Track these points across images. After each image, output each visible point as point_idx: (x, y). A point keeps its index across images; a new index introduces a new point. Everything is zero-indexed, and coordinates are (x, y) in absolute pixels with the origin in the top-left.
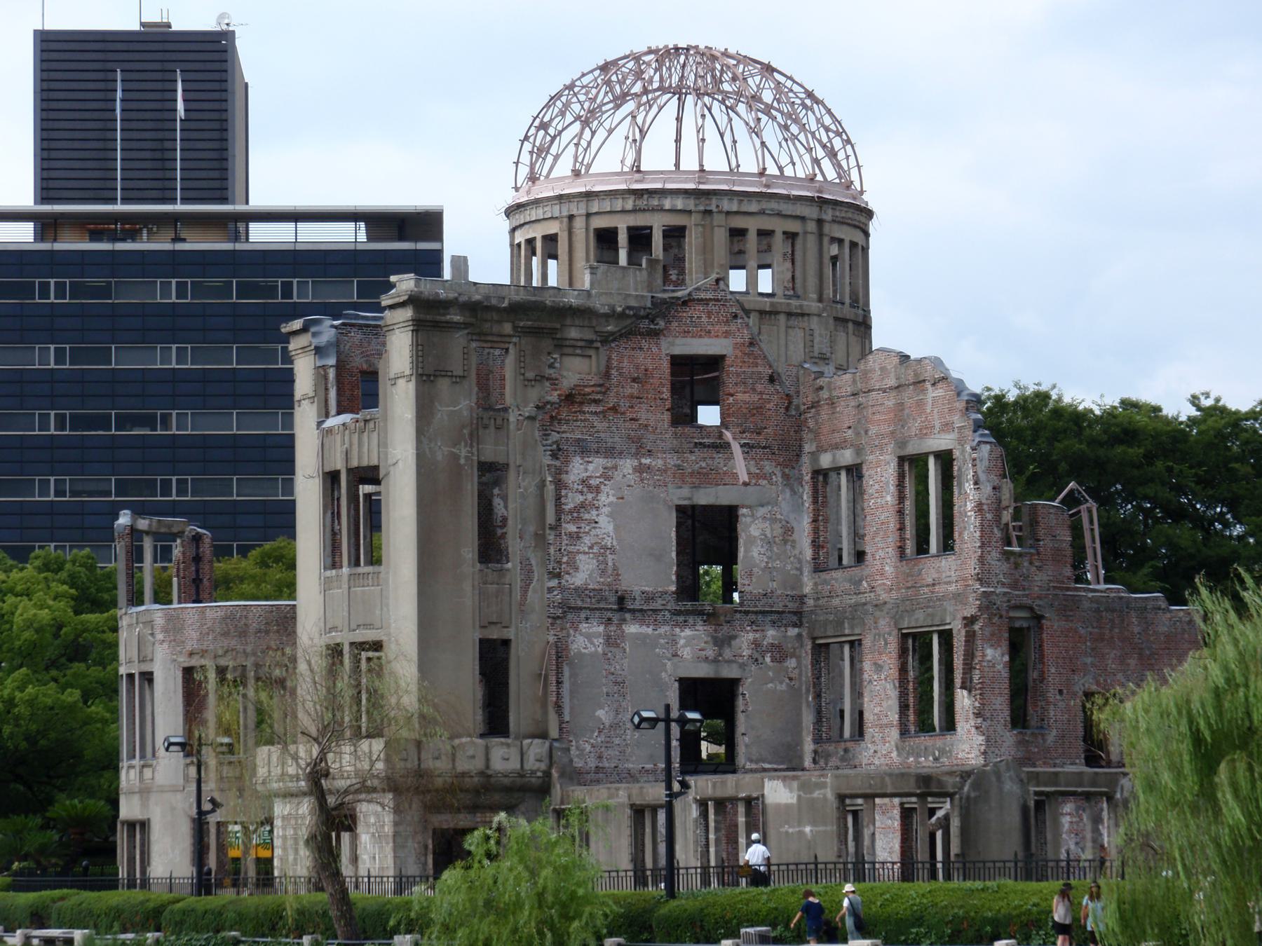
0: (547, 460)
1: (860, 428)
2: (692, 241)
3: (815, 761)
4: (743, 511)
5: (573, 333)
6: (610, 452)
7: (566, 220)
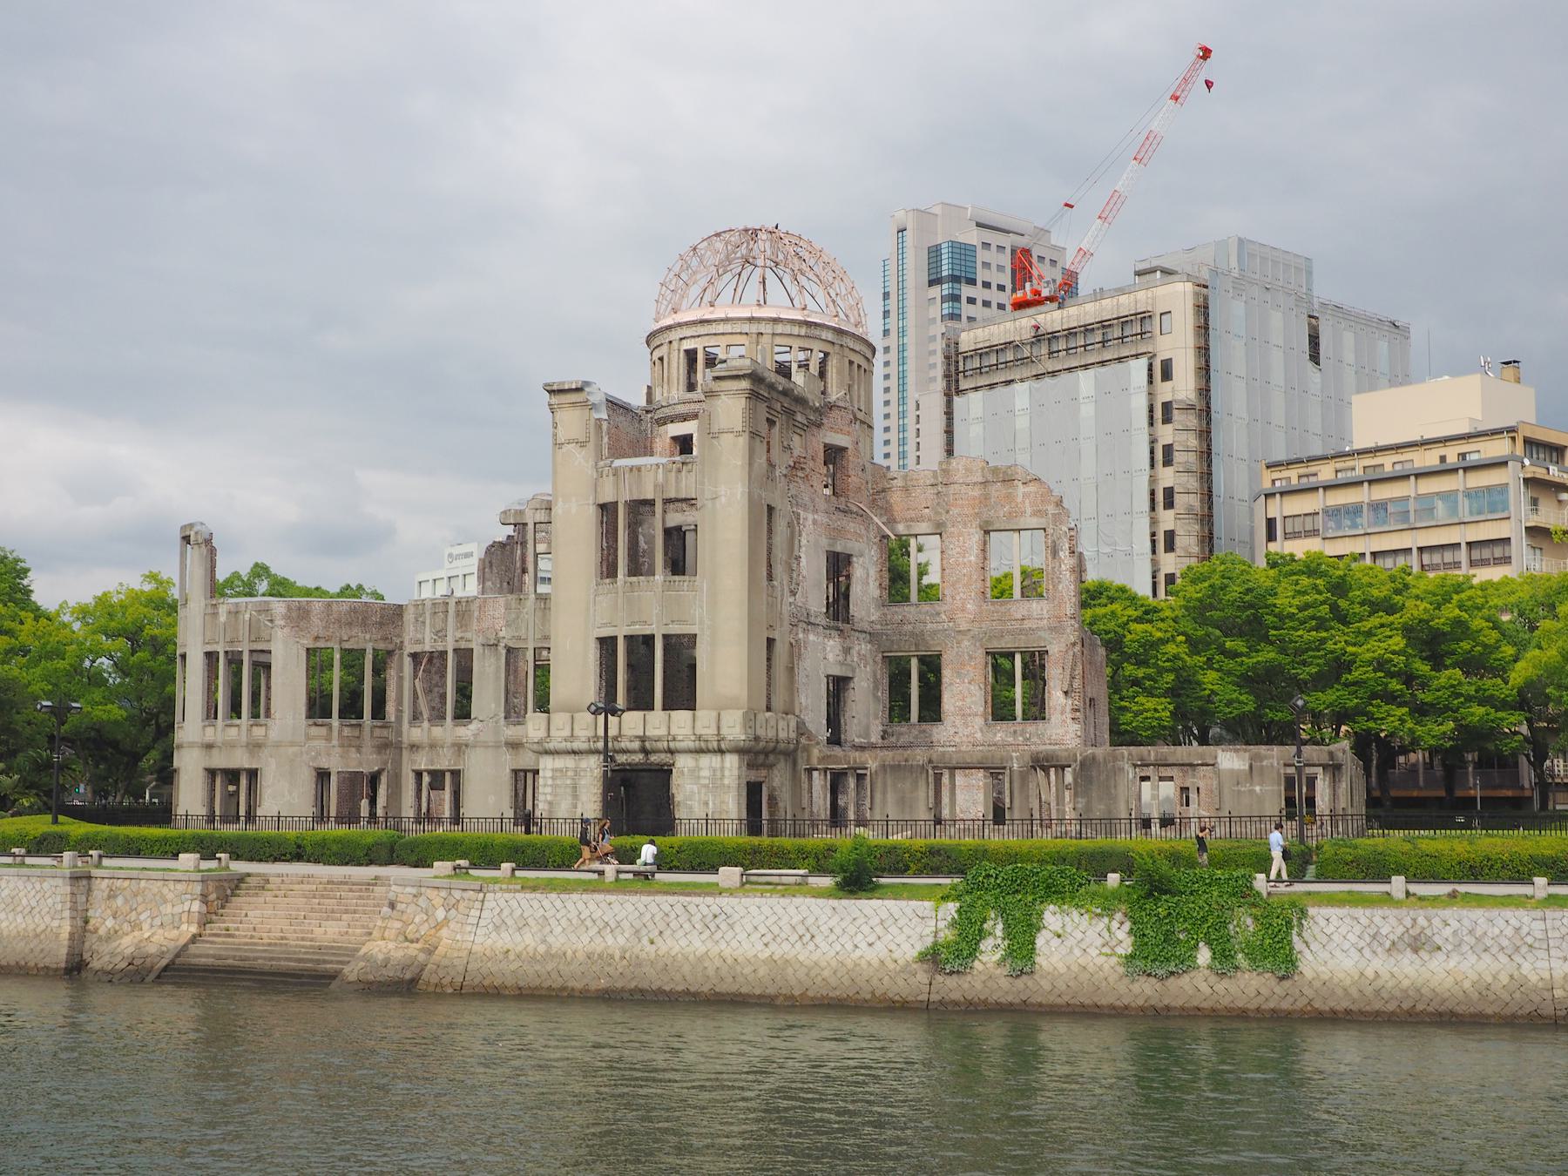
3: (883, 738)
4: (855, 559)
6: (805, 508)
7: (755, 336)
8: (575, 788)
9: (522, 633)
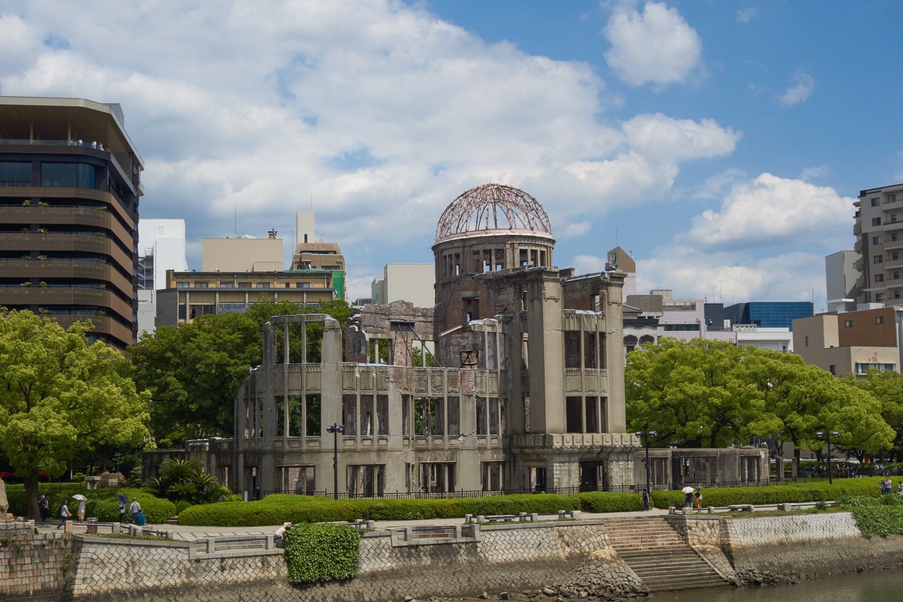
8: (569, 471)
9: (484, 390)
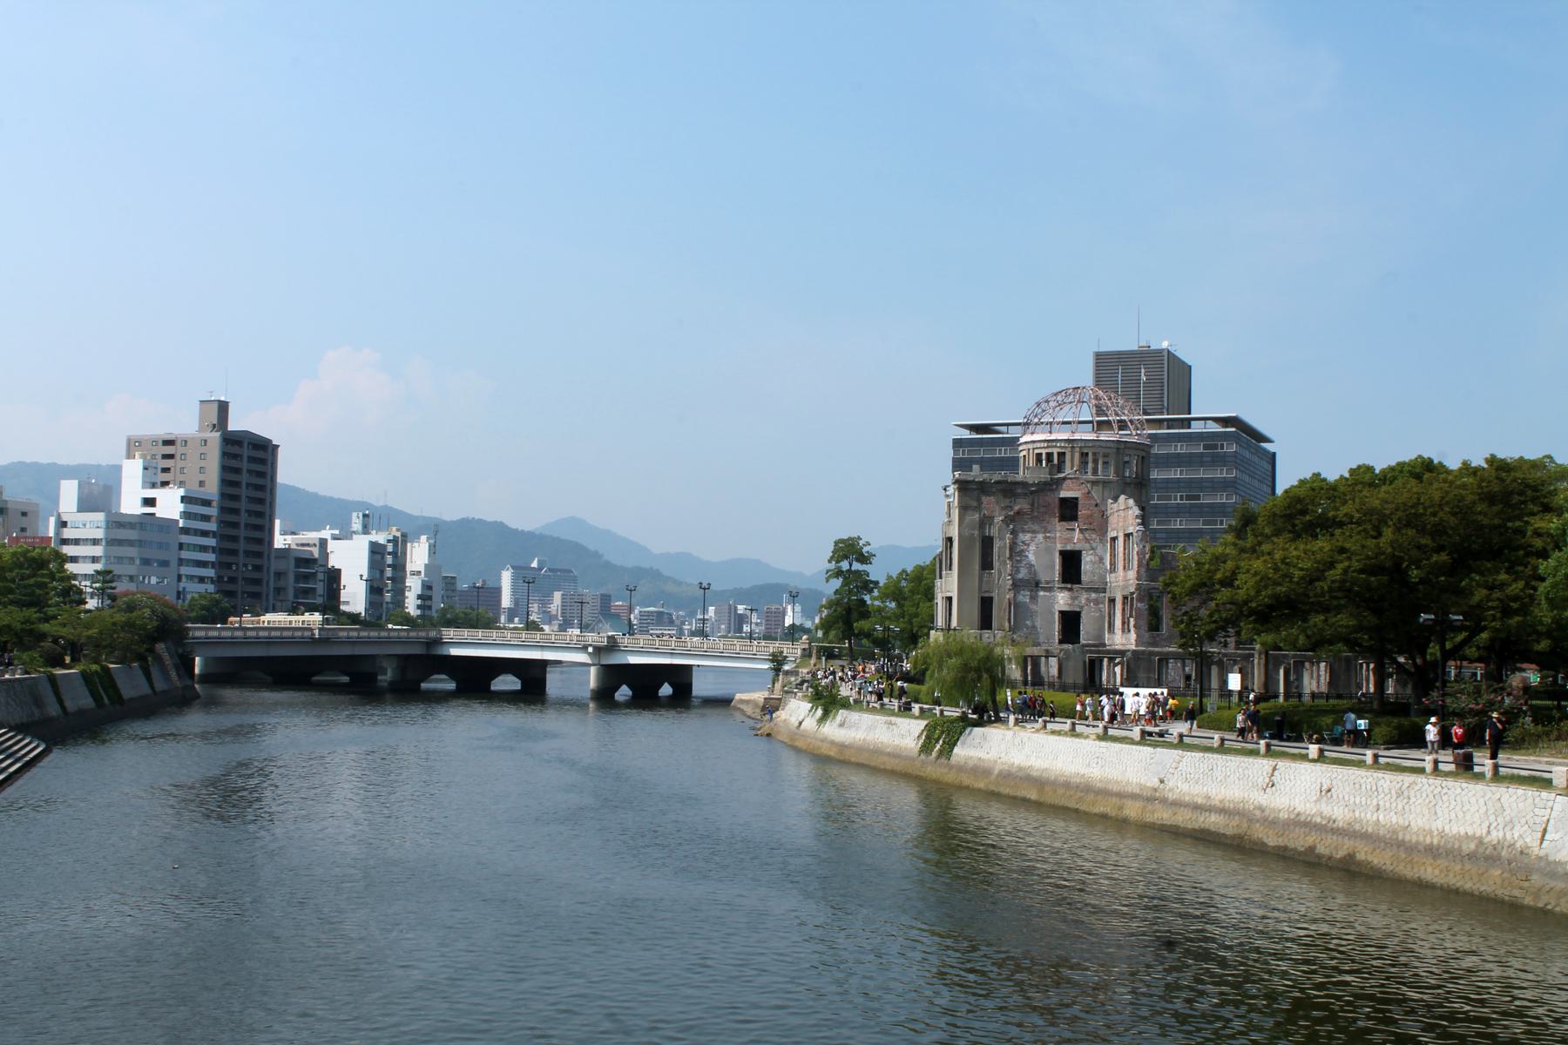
0: (1008, 536)
1: (1118, 523)
2: (1068, 457)
4: (1084, 552)
5: (1019, 491)
6: (1034, 532)
